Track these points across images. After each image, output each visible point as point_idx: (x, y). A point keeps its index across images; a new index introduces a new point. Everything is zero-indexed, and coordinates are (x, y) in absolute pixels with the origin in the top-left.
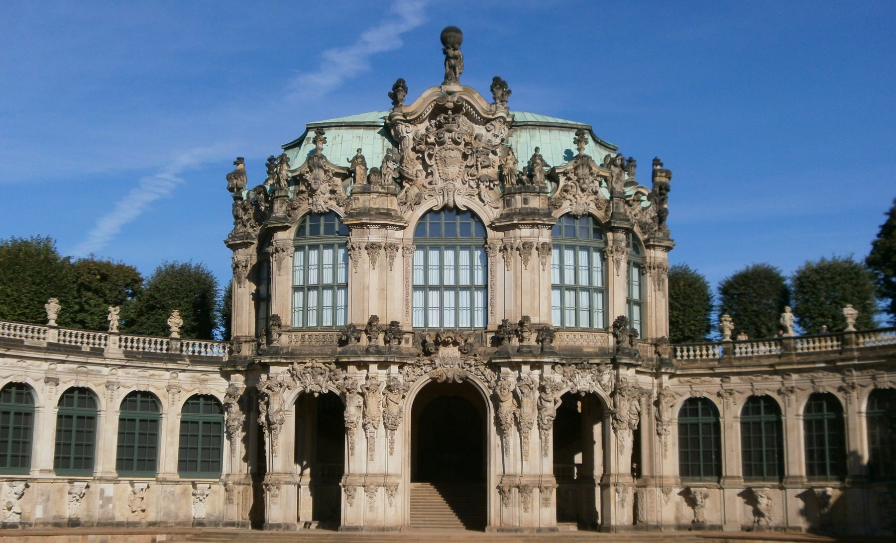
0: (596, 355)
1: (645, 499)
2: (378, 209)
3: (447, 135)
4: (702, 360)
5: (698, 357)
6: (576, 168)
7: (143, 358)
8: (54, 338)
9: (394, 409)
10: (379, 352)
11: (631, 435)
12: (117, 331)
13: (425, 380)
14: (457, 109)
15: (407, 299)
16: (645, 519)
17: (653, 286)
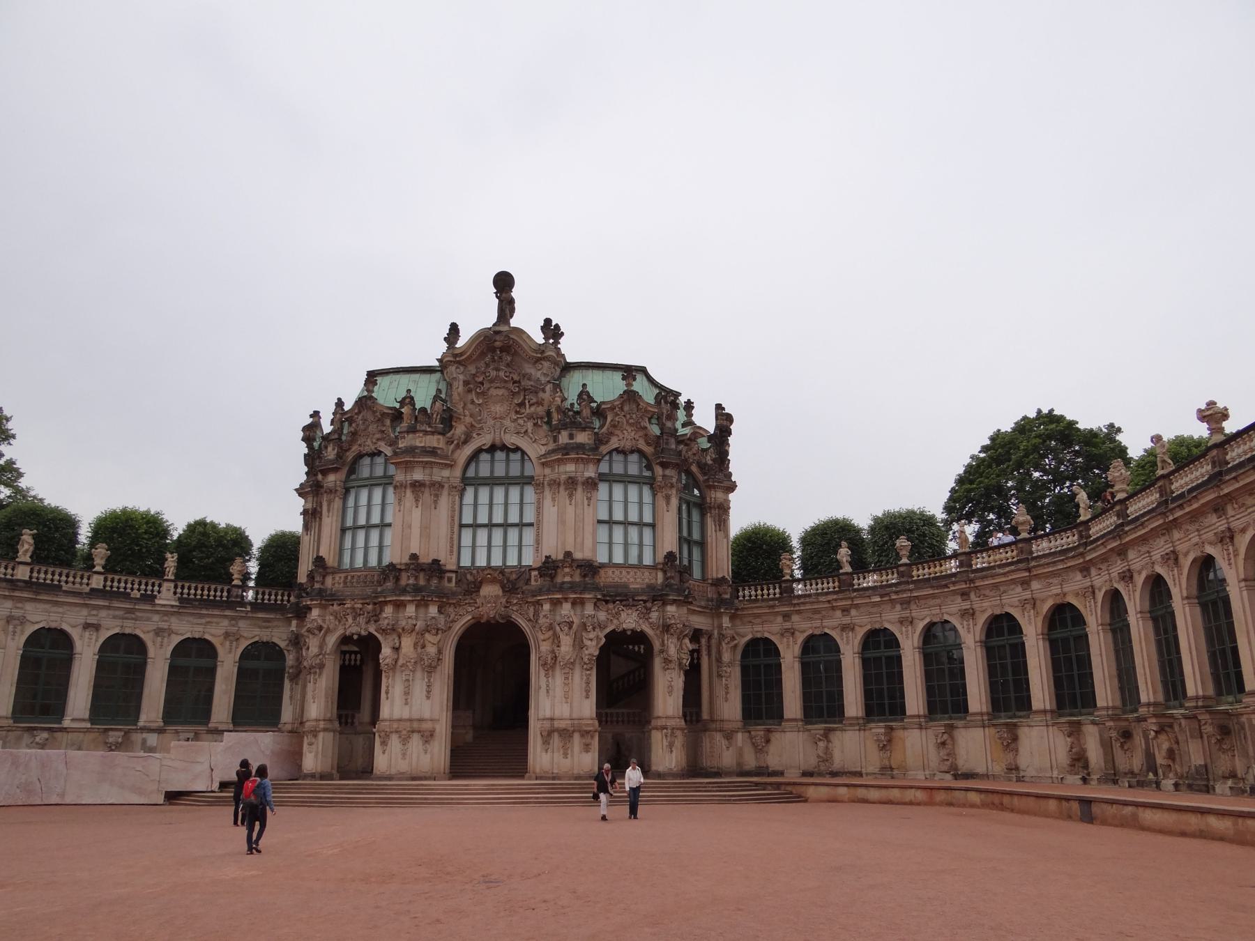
0: (643, 592)
1: (704, 744)
2: (422, 447)
3: (494, 373)
4: (763, 600)
5: (759, 597)
6: (622, 404)
7: (200, 604)
8: (98, 584)
10: (417, 589)
11: (682, 678)
12: (173, 578)
14: (502, 349)
15: (452, 538)
16: (705, 765)
17: (713, 526)
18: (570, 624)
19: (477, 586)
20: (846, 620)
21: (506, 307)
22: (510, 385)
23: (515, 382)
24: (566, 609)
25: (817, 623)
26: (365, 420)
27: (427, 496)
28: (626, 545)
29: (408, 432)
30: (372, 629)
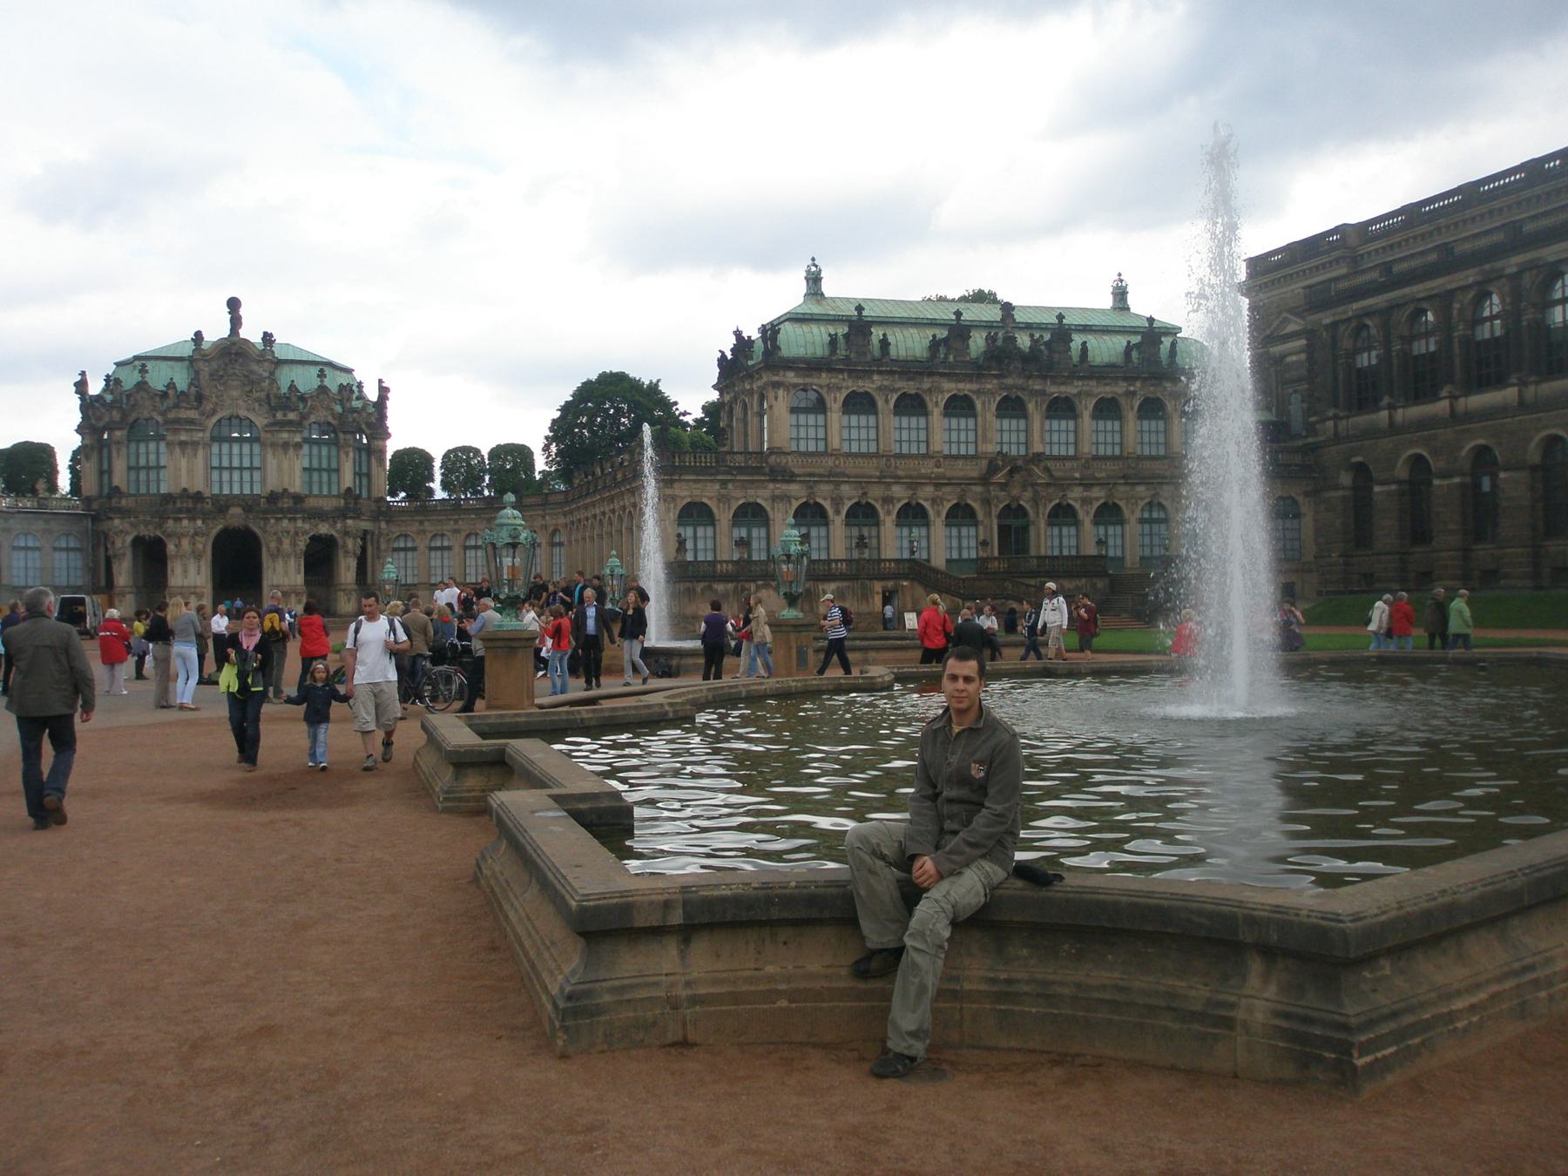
3: (231, 371)
9: (200, 546)
10: (188, 511)
11: (356, 562)
13: (220, 527)
14: (236, 354)
18: (288, 532)
19: (228, 507)
20: (456, 527)
21: (236, 322)
22: (242, 378)
23: (245, 376)
24: (285, 523)
25: (439, 528)
26: (142, 398)
27: (189, 451)
28: (320, 483)
29: (174, 408)
30: (159, 533)
